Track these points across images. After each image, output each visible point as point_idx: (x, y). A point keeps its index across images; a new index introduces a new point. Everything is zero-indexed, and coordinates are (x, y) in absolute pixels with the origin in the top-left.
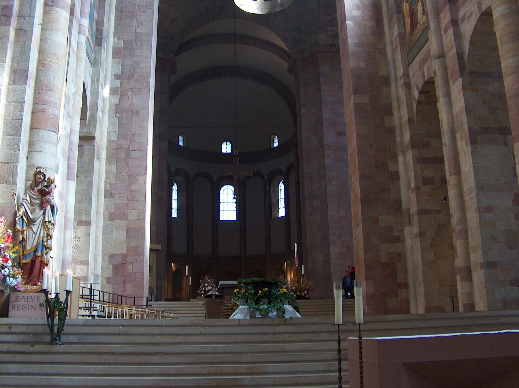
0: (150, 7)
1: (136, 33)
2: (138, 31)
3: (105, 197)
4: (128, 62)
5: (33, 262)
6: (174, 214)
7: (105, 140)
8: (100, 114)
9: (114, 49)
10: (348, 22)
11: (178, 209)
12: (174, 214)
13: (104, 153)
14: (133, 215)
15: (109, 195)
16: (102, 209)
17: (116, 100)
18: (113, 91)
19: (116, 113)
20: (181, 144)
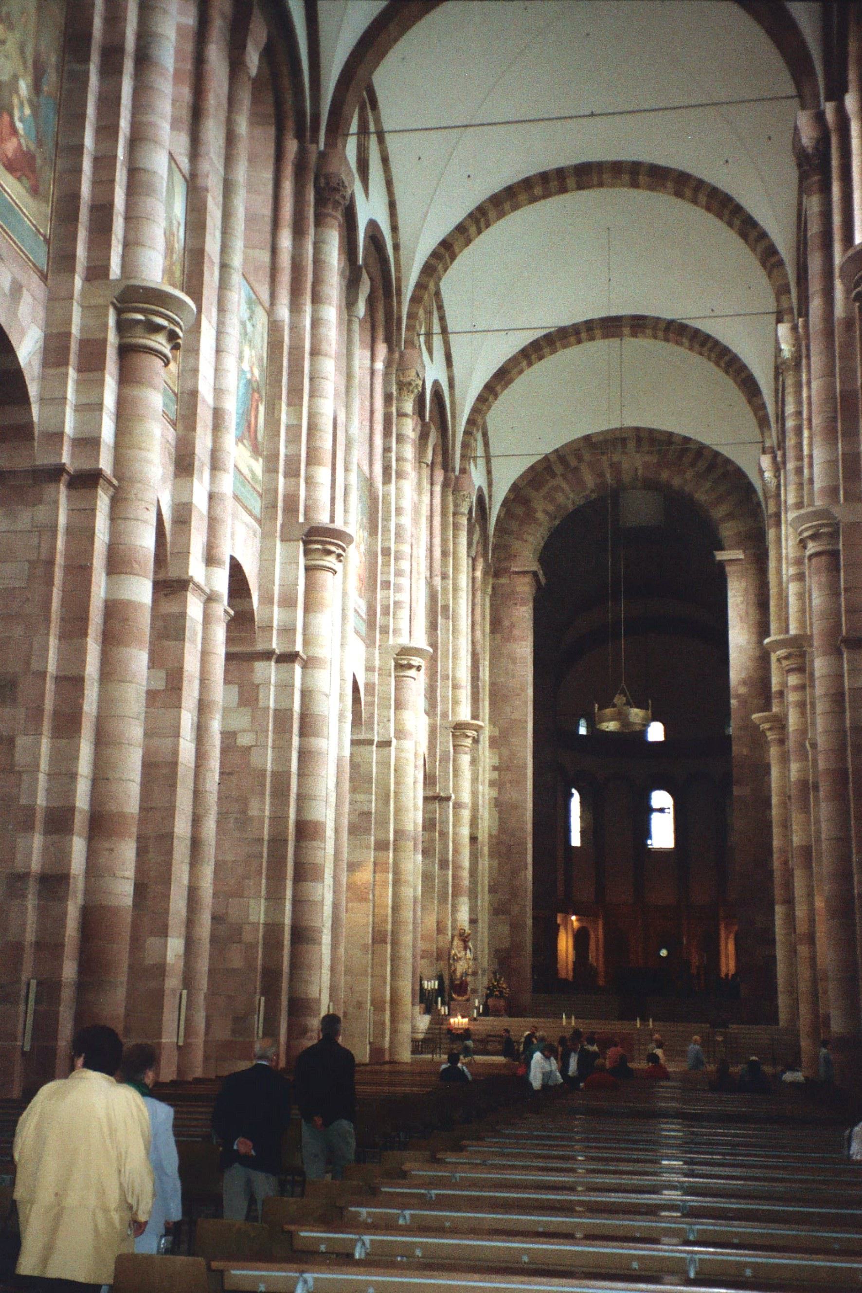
0: (523, 689)
1: (511, 719)
2: (513, 717)
3: (490, 892)
4: (505, 752)
5: (462, 983)
6: (576, 840)
7: (486, 836)
8: (481, 809)
9: (490, 737)
10: (733, 702)
11: (583, 832)
12: (576, 840)
13: (486, 849)
14: (515, 910)
15: (492, 890)
16: (486, 905)
17: (494, 793)
18: (492, 784)
19: (496, 806)
20: (583, 731)
